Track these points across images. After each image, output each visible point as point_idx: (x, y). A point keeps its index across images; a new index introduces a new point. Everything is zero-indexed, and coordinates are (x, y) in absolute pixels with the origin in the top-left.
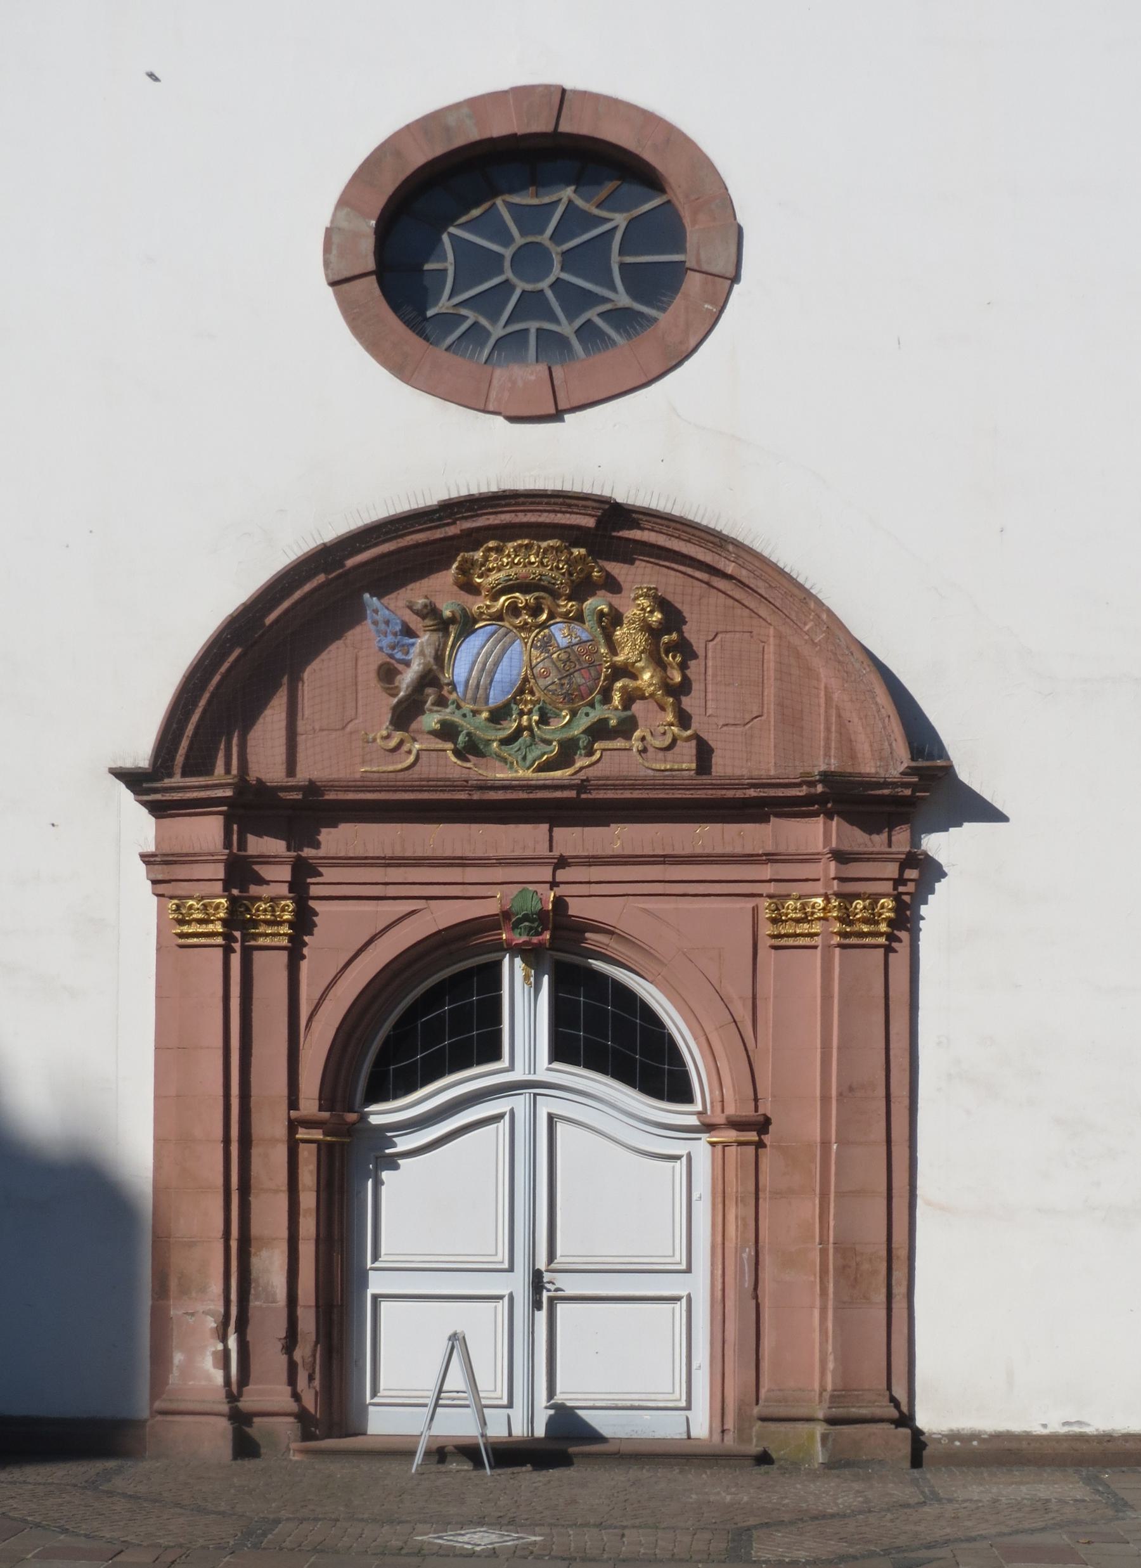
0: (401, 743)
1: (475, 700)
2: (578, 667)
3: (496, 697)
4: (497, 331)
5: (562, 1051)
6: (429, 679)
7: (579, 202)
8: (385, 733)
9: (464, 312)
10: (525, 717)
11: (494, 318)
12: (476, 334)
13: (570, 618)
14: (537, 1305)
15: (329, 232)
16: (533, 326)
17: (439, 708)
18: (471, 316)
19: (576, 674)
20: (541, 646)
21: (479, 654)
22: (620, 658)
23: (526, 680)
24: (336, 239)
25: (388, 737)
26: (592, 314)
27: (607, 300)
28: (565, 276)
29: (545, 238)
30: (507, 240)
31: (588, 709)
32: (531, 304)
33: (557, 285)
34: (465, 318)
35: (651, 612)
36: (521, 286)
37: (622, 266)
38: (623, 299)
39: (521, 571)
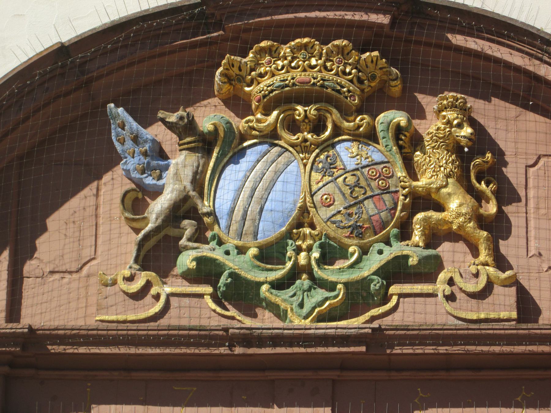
0: (148, 285)
2: (369, 193)
8: (127, 273)
10: (303, 254)
13: (359, 135)
17: (196, 245)
19: (366, 202)
20: (323, 168)
21: (246, 178)
22: (422, 182)
23: (304, 210)
25: (130, 279)
31: (381, 246)
35: (460, 126)
39: (299, 75)
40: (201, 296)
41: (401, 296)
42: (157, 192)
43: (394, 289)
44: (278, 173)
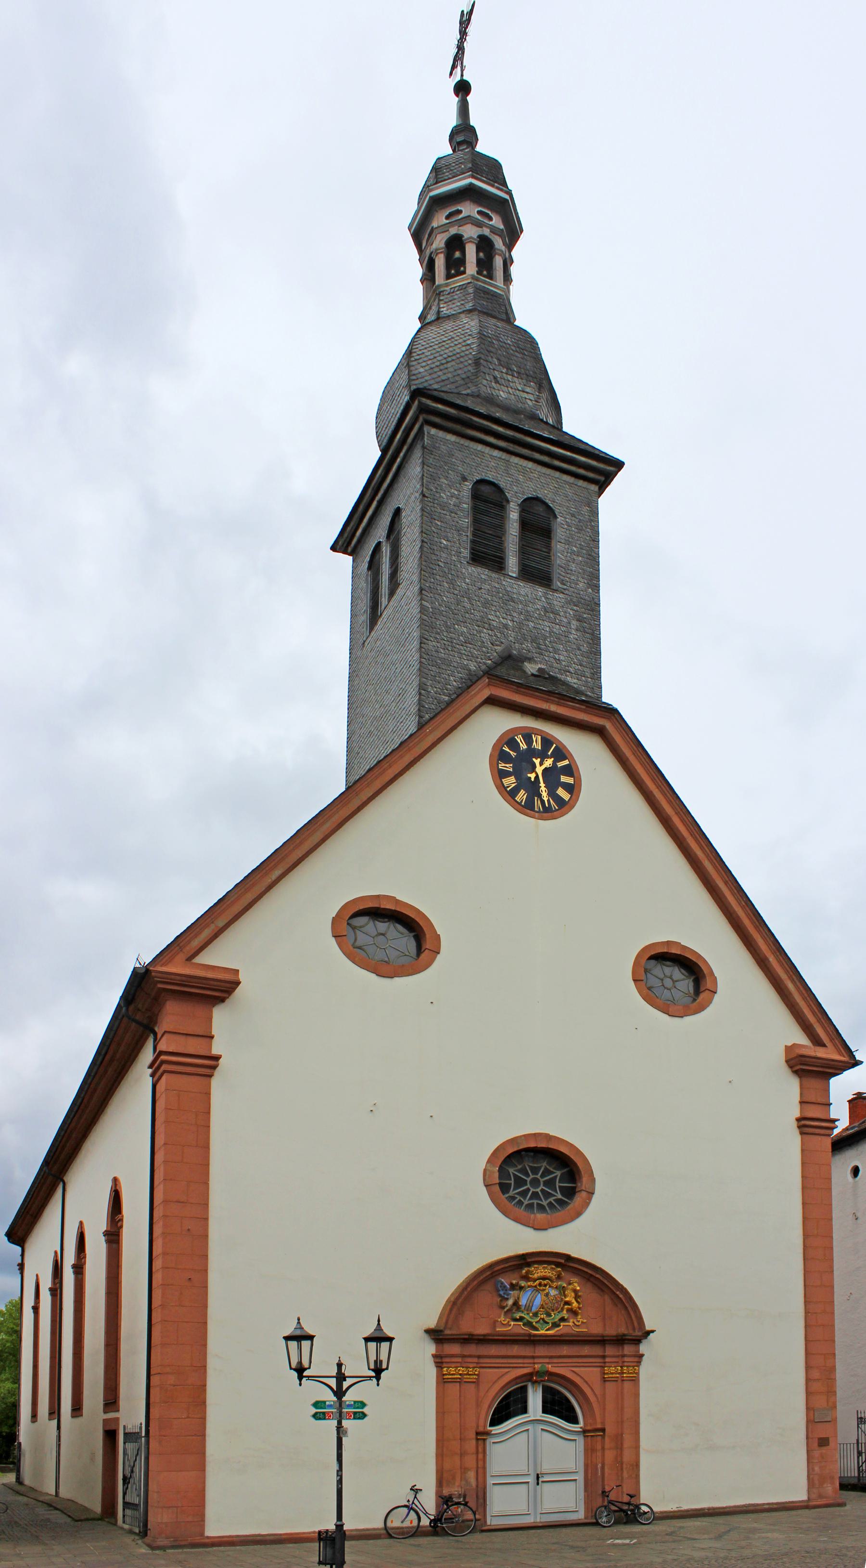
0: (509, 1322)
1: (527, 1310)
3: (534, 1309)
4: (526, 1202)
5: (545, 1411)
6: (516, 1304)
7: (548, 1167)
9: (516, 1196)
11: (525, 1199)
12: (520, 1203)
14: (538, 1484)
15: (485, 1171)
16: (535, 1202)
18: (519, 1198)
22: (567, 1299)
23: (542, 1305)
24: (488, 1173)
26: (551, 1199)
27: (555, 1196)
28: (544, 1188)
29: (538, 1176)
30: (528, 1176)
32: (535, 1195)
33: (542, 1190)
34: (517, 1198)
36: (532, 1190)
37: (559, 1186)
38: (559, 1196)
40: (520, 1325)
41: (563, 1325)
42: (507, 1299)
43: (562, 1324)
44: (537, 1296)
